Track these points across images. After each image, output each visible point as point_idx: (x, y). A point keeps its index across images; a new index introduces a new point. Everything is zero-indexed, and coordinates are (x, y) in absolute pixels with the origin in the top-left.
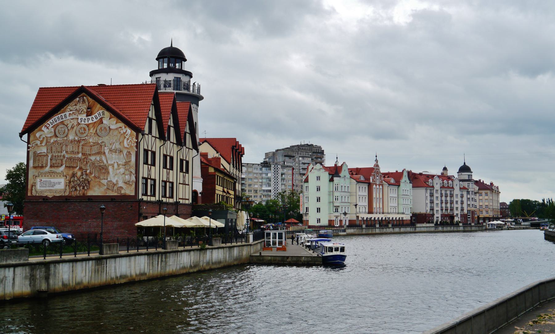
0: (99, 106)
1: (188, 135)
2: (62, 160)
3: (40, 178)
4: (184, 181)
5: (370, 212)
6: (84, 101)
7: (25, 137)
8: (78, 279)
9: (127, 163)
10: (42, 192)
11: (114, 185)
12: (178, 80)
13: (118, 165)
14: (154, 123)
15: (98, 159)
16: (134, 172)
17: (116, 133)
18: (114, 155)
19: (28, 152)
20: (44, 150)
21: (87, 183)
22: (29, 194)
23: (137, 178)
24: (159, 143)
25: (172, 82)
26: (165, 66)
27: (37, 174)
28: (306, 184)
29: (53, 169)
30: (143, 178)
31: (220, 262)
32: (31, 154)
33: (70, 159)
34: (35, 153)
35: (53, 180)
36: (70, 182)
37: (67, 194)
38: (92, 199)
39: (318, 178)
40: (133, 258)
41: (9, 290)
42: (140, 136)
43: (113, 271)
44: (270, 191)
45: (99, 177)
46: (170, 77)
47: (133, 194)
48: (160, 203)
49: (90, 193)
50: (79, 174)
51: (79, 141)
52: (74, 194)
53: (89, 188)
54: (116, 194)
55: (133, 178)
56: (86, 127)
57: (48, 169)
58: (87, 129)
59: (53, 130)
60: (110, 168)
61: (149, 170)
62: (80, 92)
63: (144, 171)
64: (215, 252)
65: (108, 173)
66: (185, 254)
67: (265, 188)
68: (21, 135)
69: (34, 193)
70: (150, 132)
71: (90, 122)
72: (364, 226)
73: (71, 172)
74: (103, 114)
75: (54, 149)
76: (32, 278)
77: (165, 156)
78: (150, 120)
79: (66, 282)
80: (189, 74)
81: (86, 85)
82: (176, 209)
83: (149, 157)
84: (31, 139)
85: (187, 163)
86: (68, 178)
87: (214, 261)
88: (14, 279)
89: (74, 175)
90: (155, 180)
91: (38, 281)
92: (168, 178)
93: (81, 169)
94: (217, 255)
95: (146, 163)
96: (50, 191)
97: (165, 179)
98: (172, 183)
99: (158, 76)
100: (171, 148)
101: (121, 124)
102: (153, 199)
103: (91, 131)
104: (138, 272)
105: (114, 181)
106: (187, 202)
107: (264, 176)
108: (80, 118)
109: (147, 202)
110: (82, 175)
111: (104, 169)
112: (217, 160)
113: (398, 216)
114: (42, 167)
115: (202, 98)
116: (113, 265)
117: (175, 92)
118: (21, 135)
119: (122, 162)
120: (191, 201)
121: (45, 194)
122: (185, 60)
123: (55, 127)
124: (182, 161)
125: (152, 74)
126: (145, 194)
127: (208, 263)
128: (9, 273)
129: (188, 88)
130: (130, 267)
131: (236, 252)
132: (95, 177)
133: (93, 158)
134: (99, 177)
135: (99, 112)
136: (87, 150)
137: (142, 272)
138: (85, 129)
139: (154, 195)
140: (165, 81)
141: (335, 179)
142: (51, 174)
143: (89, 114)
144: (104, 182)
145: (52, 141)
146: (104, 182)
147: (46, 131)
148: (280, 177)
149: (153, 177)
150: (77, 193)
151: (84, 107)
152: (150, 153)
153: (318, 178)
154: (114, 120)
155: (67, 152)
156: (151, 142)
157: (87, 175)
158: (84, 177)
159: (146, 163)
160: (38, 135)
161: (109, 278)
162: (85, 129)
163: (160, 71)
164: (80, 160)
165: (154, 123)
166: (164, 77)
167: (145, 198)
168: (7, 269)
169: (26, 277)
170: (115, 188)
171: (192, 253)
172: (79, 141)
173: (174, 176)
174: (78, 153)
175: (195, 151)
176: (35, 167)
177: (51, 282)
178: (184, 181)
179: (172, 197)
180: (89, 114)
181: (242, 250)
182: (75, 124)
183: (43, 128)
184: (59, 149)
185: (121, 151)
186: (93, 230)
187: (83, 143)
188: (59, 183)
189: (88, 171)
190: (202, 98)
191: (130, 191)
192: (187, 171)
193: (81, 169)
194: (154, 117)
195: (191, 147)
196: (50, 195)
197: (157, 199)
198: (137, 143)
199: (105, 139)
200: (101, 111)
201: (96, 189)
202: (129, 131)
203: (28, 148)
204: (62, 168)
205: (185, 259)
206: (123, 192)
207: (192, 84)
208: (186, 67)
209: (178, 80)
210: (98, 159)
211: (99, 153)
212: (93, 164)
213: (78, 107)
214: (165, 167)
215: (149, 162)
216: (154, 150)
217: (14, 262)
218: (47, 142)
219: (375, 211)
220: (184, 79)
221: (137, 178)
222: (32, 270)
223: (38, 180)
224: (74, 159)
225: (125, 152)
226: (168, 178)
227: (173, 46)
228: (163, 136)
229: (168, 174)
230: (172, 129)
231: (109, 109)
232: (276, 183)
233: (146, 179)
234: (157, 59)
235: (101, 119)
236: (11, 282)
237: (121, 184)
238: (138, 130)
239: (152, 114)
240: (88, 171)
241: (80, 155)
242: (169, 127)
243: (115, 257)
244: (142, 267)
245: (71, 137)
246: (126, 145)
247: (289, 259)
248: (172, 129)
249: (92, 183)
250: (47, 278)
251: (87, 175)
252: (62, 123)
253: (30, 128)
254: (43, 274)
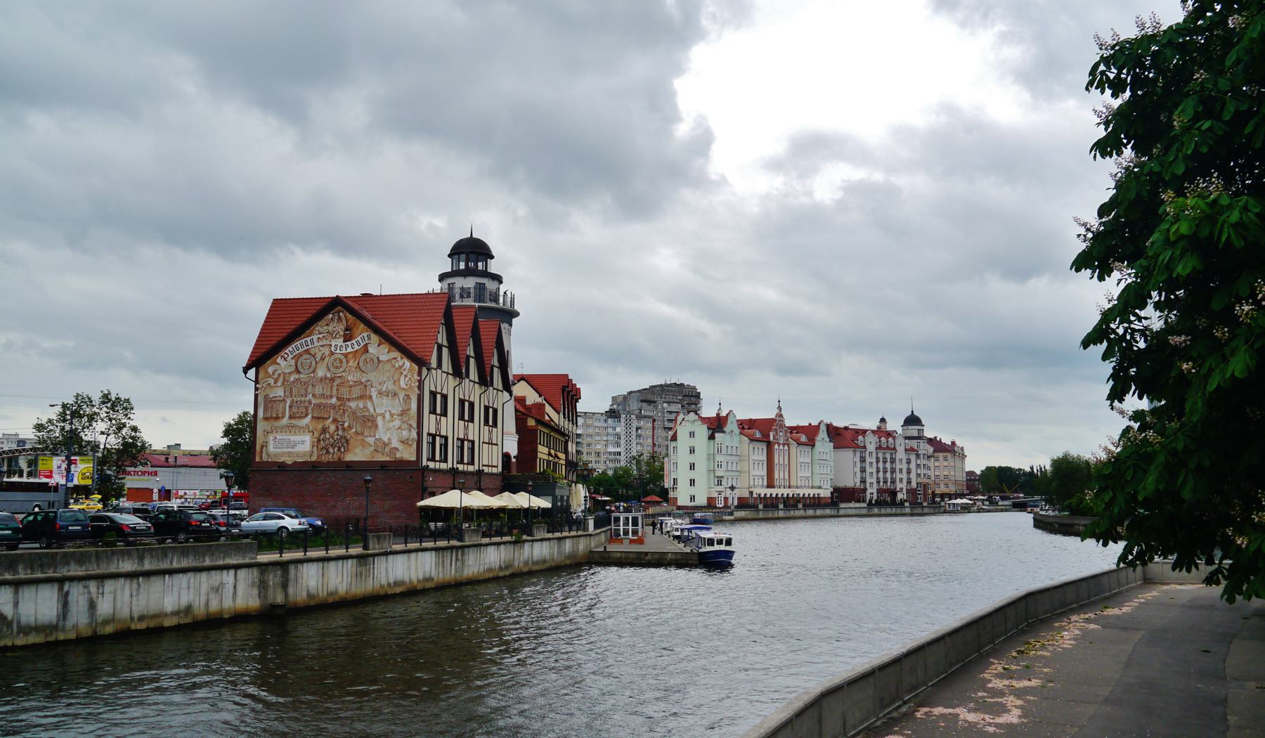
0: (362, 326)
1: (496, 370)
2: (307, 408)
3: (275, 434)
4: (490, 439)
5: (770, 485)
6: (340, 318)
7: (252, 373)
8: (332, 587)
9: (404, 413)
10: (276, 455)
11: (385, 445)
12: (481, 288)
13: (392, 415)
14: (445, 351)
15: (361, 405)
16: (415, 425)
17: (388, 366)
18: (385, 400)
19: (256, 396)
20: (280, 392)
21: (344, 443)
22: (258, 459)
23: (420, 434)
24: (452, 382)
25: (472, 291)
26: (462, 265)
27: (269, 429)
28: (673, 444)
29: (293, 421)
30: (429, 434)
31: (545, 561)
32: (261, 399)
33: (319, 406)
34: (266, 397)
35: (293, 438)
36: (319, 441)
37: (314, 458)
38: (351, 466)
39: (692, 434)
40: (413, 555)
41: (228, 603)
42: (425, 371)
43: (383, 575)
44: (619, 454)
45: (362, 434)
46: (470, 282)
47: (414, 459)
48: (454, 472)
49: (349, 457)
50: (333, 428)
51: (332, 380)
52: (325, 459)
53: (347, 450)
54: (388, 459)
55: (414, 435)
56: (342, 357)
57: (285, 421)
58: (344, 361)
59: (293, 362)
60: (379, 420)
61: (438, 423)
62: (335, 304)
63: (430, 423)
64: (537, 546)
65: (376, 426)
66: (491, 549)
67: (611, 449)
68: (246, 370)
69: (265, 458)
70: (440, 365)
71: (350, 350)
72: (761, 507)
73: (320, 426)
74: (369, 338)
75: (294, 391)
76: (263, 586)
77: (462, 402)
78: (440, 347)
79: (313, 591)
80: (498, 279)
81: (342, 294)
82: (478, 481)
83: (438, 403)
84: (261, 376)
85: (495, 411)
86: (316, 434)
87: (535, 559)
88: (235, 587)
89: (324, 430)
90: (446, 438)
91: (271, 591)
92: (466, 434)
93: (335, 420)
94: (539, 550)
95: (433, 411)
96: (289, 453)
97: (461, 436)
98: (473, 442)
99: (450, 281)
100: (470, 389)
101: (397, 354)
102: (443, 466)
103: (351, 363)
104: (421, 577)
105: (386, 439)
106: (495, 470)
107: (610, 430)
108: (333, 344)
109: (435, 471)
110: (337, 429)
111: (369, 422)
112: (540, 407)
113: (812, 492)
114: (277, 418)
115: (516, 314)
116: (384, 566)
117: (477, 304)
118: (246, 370)
119: (397, 410)
120: (500, 469)
121: (282, 460)
122: (492, 257)
123: (296, 358)
124: (487, 408)
125: (442, 278)
126: (433, 459)
127: (526, 563)
128: (228, 577)
129: (496, 300)
130: (409, 568)
131: (568, 546)
132: (357, 433)
133: (353, 404)
134: (362, 434)
135: (363, 336)
136: (344, 392)
137: (427, 575)
138: (341, 362)
139: (445, 460)
140: (462, 289)
141: (717, 435)
142: (290, 428)
143: (347, 338)
144: (371, 440)
145: (292, 379)
146: (371, 440)
147: (283, 364)
148: (634, 433)
149: (443, 433)
150: (330, 458)
151: (340, 328)
152: (439, 397)
153: (692, 434)
154: (385, 347)
155: (314, 396)
156: (440, 380)
157: (344, 430)
158: (340, 433)
159: (433, 411)
160: (270, 370)
161: (377, 585)
162: (341, 362)
163: (454, 273)
164: (333, 407)
165: (445, 351)
166: (460, 282)
167: (431, 465)
168: (225, 572)
169: (253, 584)
170: (387, 449)
171: (502, 547)
172: (332, 380)
173: (475, 431)
174: (331, 397)
175: (506, 394)
176: (266, 419)
177: (291, 591)
178: (490, 439)
179: (472, 463)
180: (347, 338)
181: (578, 543)
182: (327, 353)
183: (279, 360)
184: (303, 392)
185: (395, 394)
186: (353, 513)
187: (338, 381)
188: (303, 442)
189: (346, 425)
190: (516, 314)
191: (408, 454)
192: (495, 425)
193: (335, 420)
194: (445, 343)
195: (500, 387)
196: (289, 461)
197: (450, 465)
198: (420, 381)
199: (372, 376)
200: (365, 334)
201: (358, 451)
202: (408, 364)
203: (256, 389)
204: (307, 420)
205: (491, 557)
206: (398, 455)
207: (501, 293)
208: (494, 267)
209: (481, 288)
210: (361, 405)
211: (362, 397)
212: (354, 413)
213: (330, 328)
214: (462, 418)
215: (438, 411)
216: (445, 392)
217: (235, 562)
218: (284, 381)
219: (777, 483)
220: (490, 285)
221: (420, 434)
222: (262, 573)
223: (271, 437)
224: (325, 406)
225: (402, 395)
226: (466, 434)
228: (458, 372)
229: (466, 428)
230: (472, 361)
231: (377, 331)
232: (628, 442)
233: (434, 436)
234: (450, 256)
235: (366, 346)
236: (232, 590)
237: (395, 444)
238: (421, 363)
239: (442, 338)
240: (346, 425)
241: (334, 400)
242: (468, 357)
243: (386, 554)
244: (428, 569)
245: (321, 373)
246: (403, 384)
247: (649, 557)
248: (472, 361)
249: (352, 442)
250: (285, 586)
251: (344, 430)
252: (307, 352)
253: (259, 360)
254: (278, 579)
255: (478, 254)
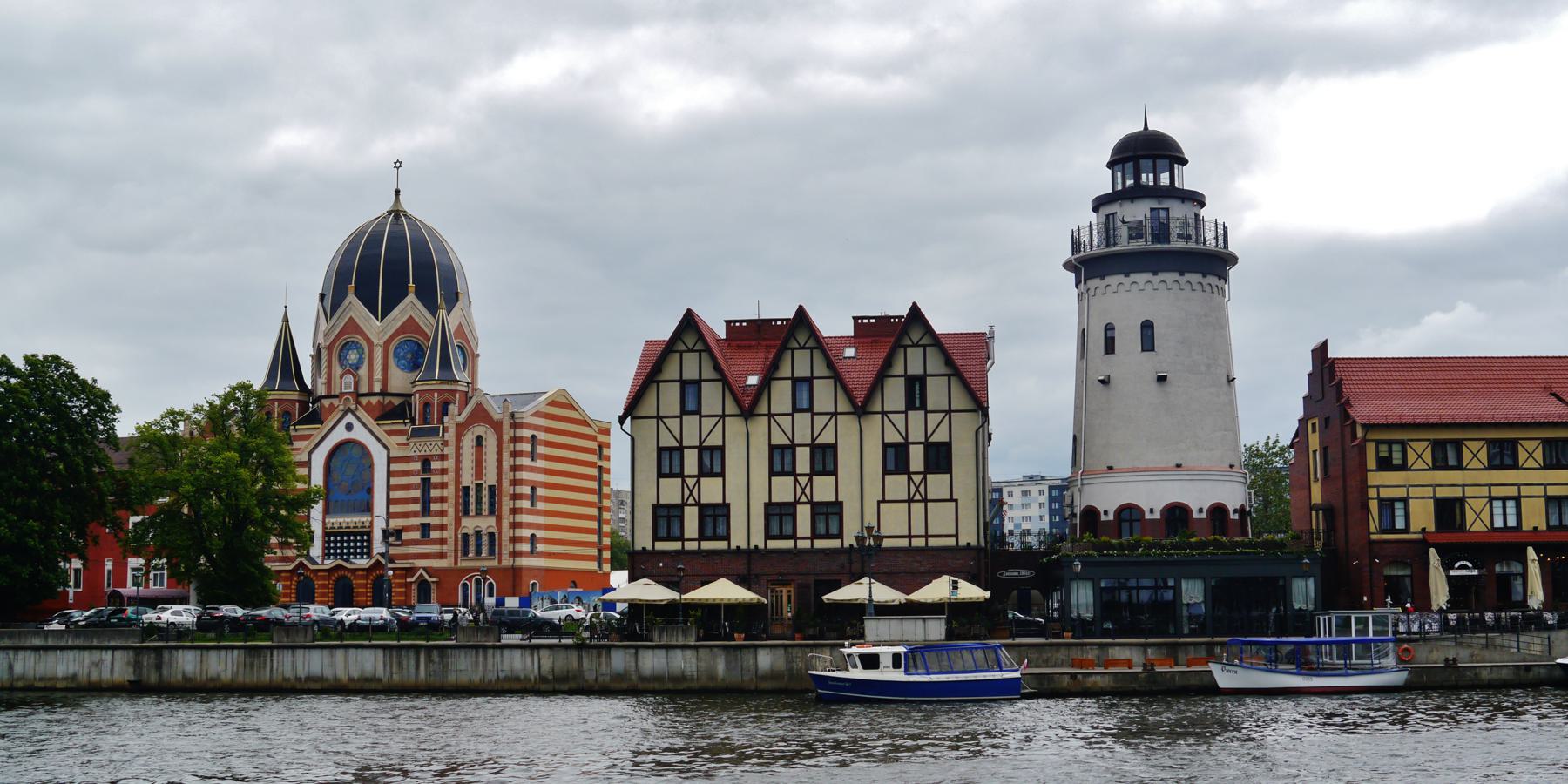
76: (137, 665)
80: (1197, 199)
91: (145, 670)
115: (1233, 260)
122: (1184, 162)
169: (128, 663)
177: (165, 672)
190: (1233, 260)
208: (1189, 178)
217: (113, 644)
220: (1178, 211)
222: (137, 655)
227: (1150, 128)
250: (159, 667)
254: (152, 661)
255: (1154, 158)
